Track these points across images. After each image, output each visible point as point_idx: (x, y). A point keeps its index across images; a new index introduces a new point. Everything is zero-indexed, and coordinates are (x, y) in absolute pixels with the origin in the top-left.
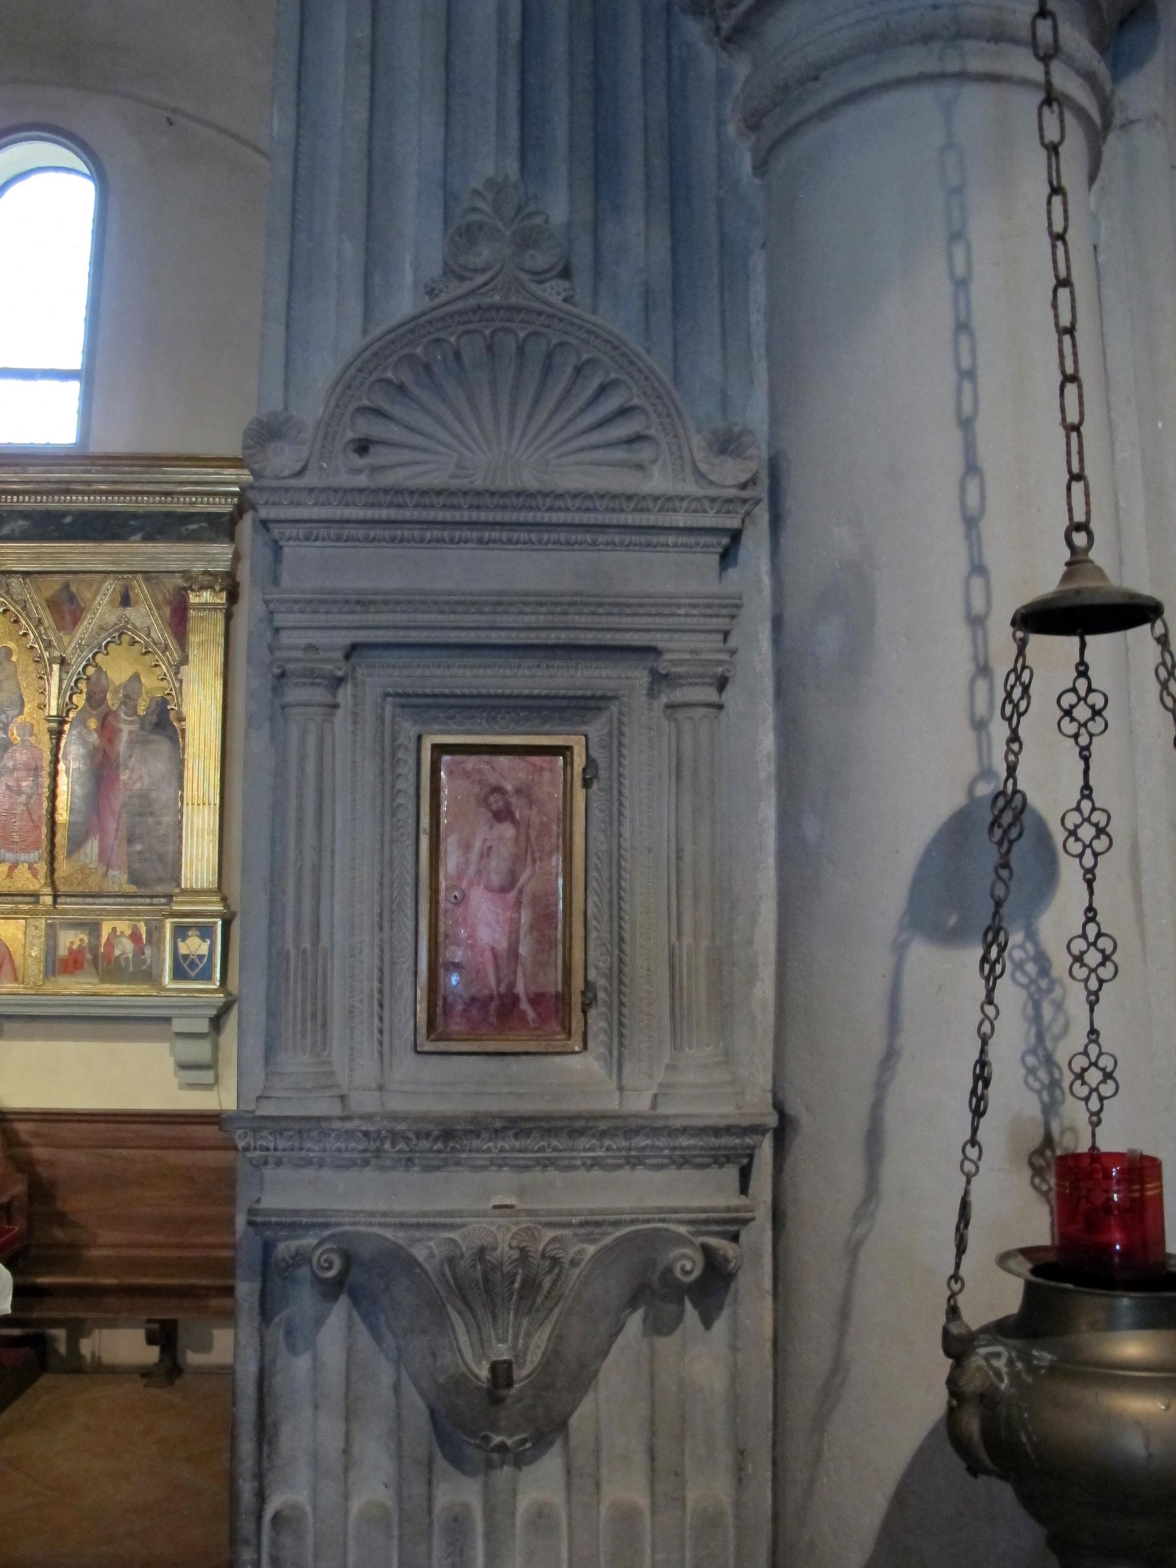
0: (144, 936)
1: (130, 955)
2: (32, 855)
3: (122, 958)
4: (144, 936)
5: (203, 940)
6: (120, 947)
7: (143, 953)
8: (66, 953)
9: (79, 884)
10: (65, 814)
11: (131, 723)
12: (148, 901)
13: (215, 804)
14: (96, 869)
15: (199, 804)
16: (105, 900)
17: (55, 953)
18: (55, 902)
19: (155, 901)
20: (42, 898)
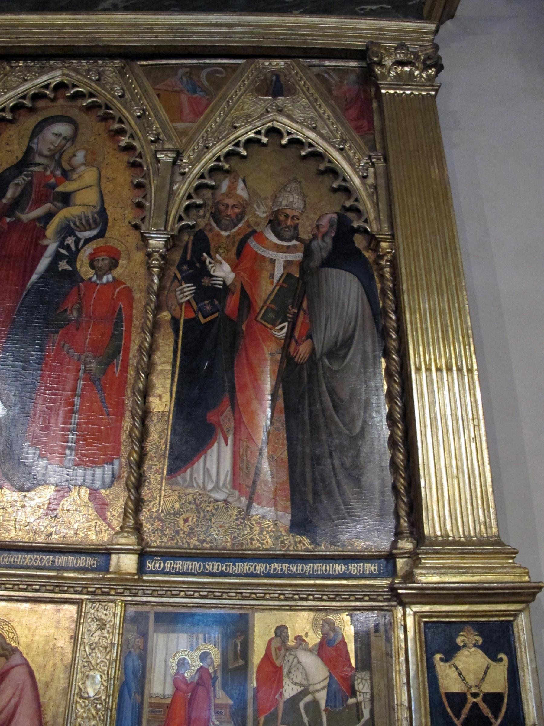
0: (351, 647)
1: (322, 697)
2: (98, 472)
3: (302, 705)
4: (351, 647)
5: (494, 658)
6: (298, 677)
7: (353, 693)
8: (169, 690)
9: (191, 533)
10: (166, 398)
11: (288, 250)
12: (339, 568)
13: (470, 371)
14: (226, 501)
15: (449, 369)
16: (247, 567)
17: (142, 692)
18: (141, 568)
19: (354, 568)
20: (114, 558)
